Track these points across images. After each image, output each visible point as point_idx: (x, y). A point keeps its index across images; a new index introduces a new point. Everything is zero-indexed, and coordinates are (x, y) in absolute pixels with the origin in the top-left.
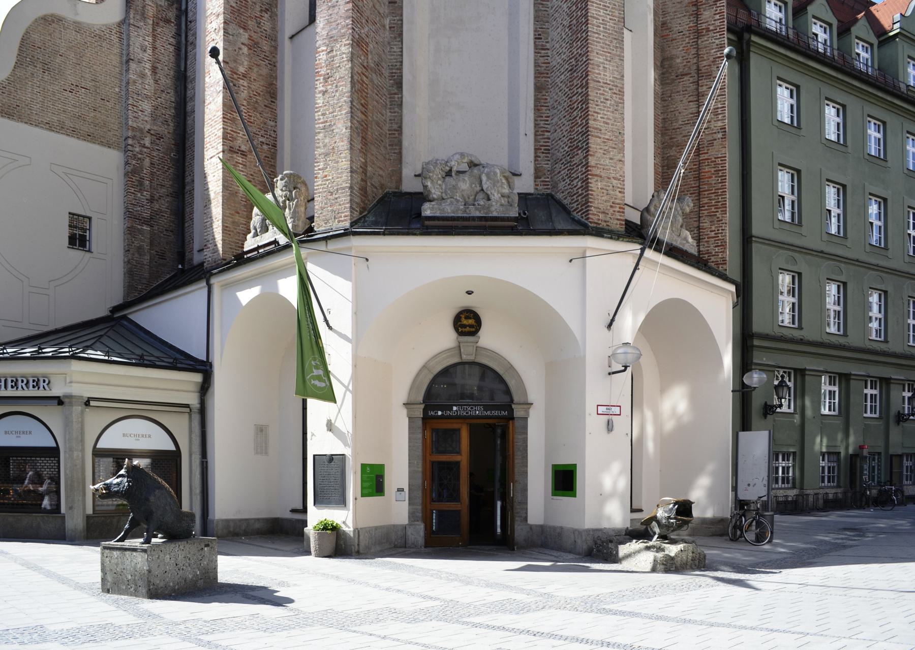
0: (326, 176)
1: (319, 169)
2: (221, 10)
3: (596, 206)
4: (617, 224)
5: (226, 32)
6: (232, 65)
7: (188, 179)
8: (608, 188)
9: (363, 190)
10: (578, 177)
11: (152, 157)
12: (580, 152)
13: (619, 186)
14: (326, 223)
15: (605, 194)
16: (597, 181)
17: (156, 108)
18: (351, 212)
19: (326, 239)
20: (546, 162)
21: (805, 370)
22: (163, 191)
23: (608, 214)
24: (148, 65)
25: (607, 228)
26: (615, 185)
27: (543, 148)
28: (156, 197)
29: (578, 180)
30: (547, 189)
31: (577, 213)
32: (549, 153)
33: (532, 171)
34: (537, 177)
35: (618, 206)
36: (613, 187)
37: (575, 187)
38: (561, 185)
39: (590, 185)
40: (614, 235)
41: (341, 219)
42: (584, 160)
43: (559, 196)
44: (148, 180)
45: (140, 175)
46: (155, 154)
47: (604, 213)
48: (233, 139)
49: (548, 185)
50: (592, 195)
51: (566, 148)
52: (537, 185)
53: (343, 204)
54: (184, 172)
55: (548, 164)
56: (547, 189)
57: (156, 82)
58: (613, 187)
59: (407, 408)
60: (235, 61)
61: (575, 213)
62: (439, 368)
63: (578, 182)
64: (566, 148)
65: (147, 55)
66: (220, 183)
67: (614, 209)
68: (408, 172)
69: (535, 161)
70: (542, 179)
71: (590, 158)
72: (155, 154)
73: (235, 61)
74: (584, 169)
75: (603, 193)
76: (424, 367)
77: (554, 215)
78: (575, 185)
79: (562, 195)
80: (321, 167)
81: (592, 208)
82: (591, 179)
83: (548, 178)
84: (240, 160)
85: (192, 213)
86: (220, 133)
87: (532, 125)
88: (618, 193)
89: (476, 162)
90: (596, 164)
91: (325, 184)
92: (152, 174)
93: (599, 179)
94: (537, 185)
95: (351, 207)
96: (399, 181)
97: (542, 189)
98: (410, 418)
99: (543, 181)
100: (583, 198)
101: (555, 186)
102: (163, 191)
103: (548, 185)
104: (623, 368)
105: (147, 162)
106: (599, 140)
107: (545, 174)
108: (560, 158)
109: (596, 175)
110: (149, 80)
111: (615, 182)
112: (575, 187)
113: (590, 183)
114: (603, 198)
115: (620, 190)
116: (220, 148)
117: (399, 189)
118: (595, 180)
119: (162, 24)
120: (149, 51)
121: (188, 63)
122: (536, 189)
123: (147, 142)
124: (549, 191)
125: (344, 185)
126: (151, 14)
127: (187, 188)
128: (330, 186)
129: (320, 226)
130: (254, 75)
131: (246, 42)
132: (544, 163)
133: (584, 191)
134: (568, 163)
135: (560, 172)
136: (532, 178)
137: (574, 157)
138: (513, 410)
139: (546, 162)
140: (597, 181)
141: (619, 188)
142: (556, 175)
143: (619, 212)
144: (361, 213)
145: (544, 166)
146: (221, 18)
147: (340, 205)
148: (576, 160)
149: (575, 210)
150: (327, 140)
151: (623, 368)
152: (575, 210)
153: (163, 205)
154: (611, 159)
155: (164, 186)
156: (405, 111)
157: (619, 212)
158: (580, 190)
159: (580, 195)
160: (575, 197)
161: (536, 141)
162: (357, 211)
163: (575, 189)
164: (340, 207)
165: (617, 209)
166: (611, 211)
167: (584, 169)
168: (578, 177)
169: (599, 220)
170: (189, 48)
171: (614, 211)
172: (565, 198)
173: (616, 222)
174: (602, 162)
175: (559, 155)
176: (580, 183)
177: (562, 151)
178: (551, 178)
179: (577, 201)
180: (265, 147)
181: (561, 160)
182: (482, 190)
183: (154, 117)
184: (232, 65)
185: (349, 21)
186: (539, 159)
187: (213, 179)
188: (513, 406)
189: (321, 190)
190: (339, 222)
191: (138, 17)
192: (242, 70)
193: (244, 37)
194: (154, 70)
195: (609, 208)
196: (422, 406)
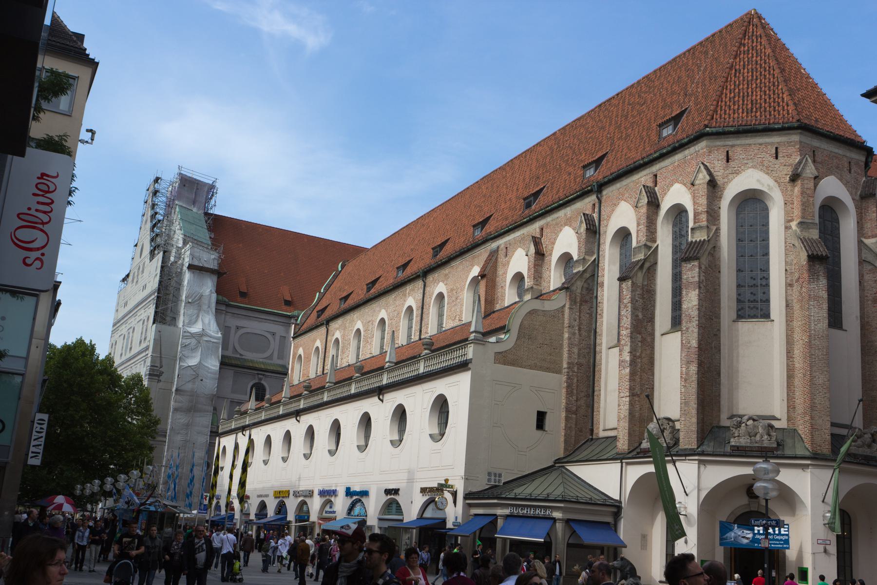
2: (629, 327)
5: (631, 338)
6: (634, 353)
11: (577, 377)
17: (580, 350)
19: (686, 455)
24: (577, 328)
43: (800, 432)
46: (579, 374)
48: (634, 389)
57: (580, 335)
60: (635, 351)
62: (739, 513)
65: (576, 323)
66: (627, 411)
68: (724, 416)
72: (579, 374)
73: (635, 351)
76: (732, 513)
77: (796, 443)
84: (637, 399)
86: (628, 387)
87: (786, 395)
96: (719, 421)
97: (791, 426)
105: (575, 380)
106: (816, 412)
110: (577, 336)
116: (628, 394)
119: (583, 304)
120: (578, 320)
121: (598, 324)
123: (576, 369)
125: (694, 429)
126: (578, 300)
127: (596, 393)
130: (643, 355)
131: (640, 340)
146: (629, 331)
150: (686, 408)
153: (582, 402)
156: (722, 387)
161: (788, 402)
170: (598, 317)
175: (800, 412)
180: (648, 390)
183: (579, 355)
184: (634, 353)
185: (696, 356)
191: (573, 303)
192: (638, 354)
193: (639, 337)
194: (580, 330)
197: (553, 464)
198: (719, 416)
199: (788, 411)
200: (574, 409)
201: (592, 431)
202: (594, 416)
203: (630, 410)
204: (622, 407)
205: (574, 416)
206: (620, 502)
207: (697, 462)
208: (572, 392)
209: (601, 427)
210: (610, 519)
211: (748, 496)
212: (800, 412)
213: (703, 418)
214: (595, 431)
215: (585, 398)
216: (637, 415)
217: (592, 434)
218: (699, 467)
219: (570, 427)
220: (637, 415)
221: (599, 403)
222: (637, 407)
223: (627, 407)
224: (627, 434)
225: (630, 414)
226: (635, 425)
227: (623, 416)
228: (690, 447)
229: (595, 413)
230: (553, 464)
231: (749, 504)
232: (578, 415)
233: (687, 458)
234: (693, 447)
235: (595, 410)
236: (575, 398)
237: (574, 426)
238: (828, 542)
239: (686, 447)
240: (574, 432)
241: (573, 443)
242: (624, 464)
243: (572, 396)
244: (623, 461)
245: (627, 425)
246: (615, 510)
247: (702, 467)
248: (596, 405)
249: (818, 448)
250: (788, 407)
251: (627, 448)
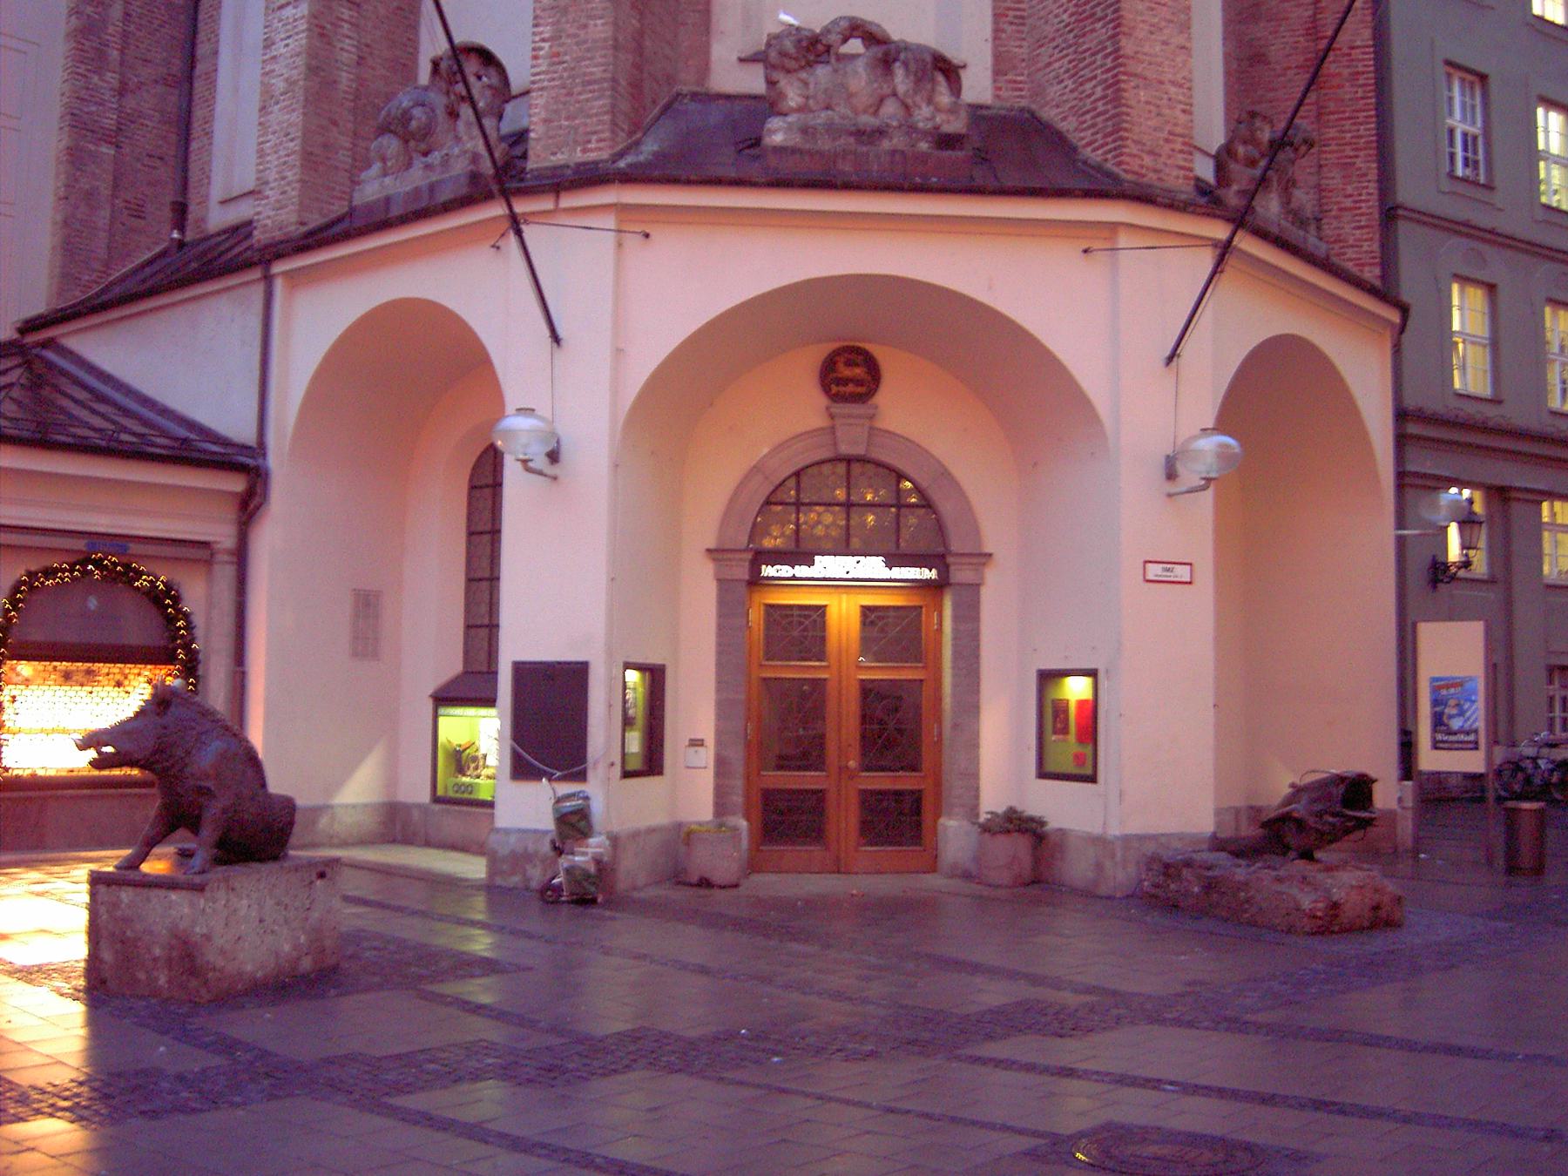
0: (557, 55)
1: (543, 40)
3: (1135, 137)
4: (1178, 177)
7: (202, 50)
8: (1158, 102)
9: (636, 86)
10: (1095, 77)
12: (1099, 25)
13: (1181, 98)
14: (554, 154)
15: (1153, 115)
16: (1137, 87)
18: (613, 132)
20: (1018, 43)
21: (1510, 489)
22: (146, 73)
23: (1160, 156)
25: (1158, 184)
26: (1174, 96)
27: (1011, 13)
28: (131, 85)
29: (1094, 82)
30: (1021, 97)
31: (1094, 150)
32: (1023, 24)
33: (988, 59)
34: (998, 72)
35: (1181, 139)
36: (1170, 99)
37: (1089, 96)
38: (1054, 91)
39: (1125, 94)
40: (1173, 205)
41: (589, 146)
42: (1108, 43)
44: (117, 49)
45: (99, 38)
47: (1151, 153)
49: (1021, 90)
50: (1128, 115)
51: (1065, 17)
52: (1000, 89)
53: (596, 115)
54: (195, 33)
55: (1021, 47)
56: (1021, 97)
58: (1170, 99)
59: (714, 560)
61: (1089, 149)
63: (1095, 86)
64: (1065, 17)
66: (300, 61)
67: (1172, 146)
69: (995, 38)
70: (1009, 77)
71: (1124, 42)
74: (1109, 60)
75: (1150, 112)
76: (756, 469)
78: (1090, 91)
79: (1055, 111)
80: (546, 35)
81: (1129, 142)
82: (1124, 81)
83: (1023, 75)
84: (346, 14)
85: (209, 120)
88: (1178, 113)
89: (879, 35)
90: (1136, 53)
91: (556, 72)
92: (125, 35)
93: (1141, 82)
94: (1000, 89)
95: (614, 123)
96: (705, 69)
98: (719, 581)
99: (1010, 82)
100: (1107, 120)
101: (1039, 91)
102: (146, 73)
103: (1021, 90)
104: (1203, 482)
107: (1015, 67)
108: (1051, 36)
109: (1135, 75)
111: (1173, 90)
112: (1089, 96)
113: (1125, 90)
114: (1149, 123)
115: (1185, 107)
117: (703, 85)
118: (1132, 84)
122: (998, 97)
124: (1024, 103)
125: (597, 72)
127: (200, 68)
128: (565, 75)
129: (540, 157)
132: (1012, 43)
133: (1109, 106)
134: (1070, 46)
135: (1049, 64)
136: (989, 73)
137: (1084, 35)
138: (947, 566)
139: (1018, 43)
140: (1137, 87)
141: (1180, 102)
142: (1039, 70)
143: (1181, 151)
144: (631, 133)
145: (1017, 50)
147: (590, 116)
148: (1090, 42)
149: (1089, 144)
151: (1203, 482)
152: (1089, 144)
154: (1165, 43)
155: (150, 62)
157: (1181, 151)
158: (1100, 104)
159: (1099, 114)
160: (1088, 116)
162: (623, 130)
163: (1089, 101)
164: (588, 121)
165: (1178, 147)
166: (1167, 148)
167: (1109, 60)
168: (1095, 77)
169: (1142, 167)
171: (1173, 150)
172: (1064, 119)
173: (1175, 173)
174: (1146, 49)
175: (1049, 30)
176: (1099, 89)
177: (1056, 20)
178: (1029, 75)
179: (1093, 125)
181: (1053, 39)
182: (895, 94)
186: (1004, 35)
187: (283, 50)
188: (950, 560)
189: (546, 84)
190: (584, 151)
195: (1161, 142)
196: (749, 556)
197: (16, 336)
198: (704, 51)
199: (997, 31)
200: (110, 121)
201: (180, 212)
202: (193, 157)
203: (312, 53)
204: (279, 49)
205: (107, 150)
206: (261, 448)
207: (610, 221)
208: (101, 56)
209: (217, 191)
210: (222, 534)
211: (826, 388)
212: (1049, 30)
213: (639, 36)
214: (194, 212)
215: (160, 89)
216: (345, 79)
217: (180, 223)
218: (620, 245)
219: (90, 195)
220: (345, 79)
221: (210, 101)
222: (346, 49)
223: (300, 41)
224: (295, 160)
225: (313, 70)
226: (335, 123)
227: (279, 85)
228: (579, 156)
229: (194, 146)
230: (16, 336)
231: (833, 429)
232: (126, 150)
233: (568, 201)
234: (592, 156)
235: (197, 129)
236: (112, 78)
237: (105, 190)
238: (1182, 573)
239: (560, 158)
240: (105, 213)
241: (102, 253)
242: (279, 286)
243: (99, 71)
244: (278, 268)
245: (296, 117)
246: (236, 484)
247: (632, 242)
248: (199, 113)
249: (1148, 161)
250: (997, 16)
251: (294, 218)
